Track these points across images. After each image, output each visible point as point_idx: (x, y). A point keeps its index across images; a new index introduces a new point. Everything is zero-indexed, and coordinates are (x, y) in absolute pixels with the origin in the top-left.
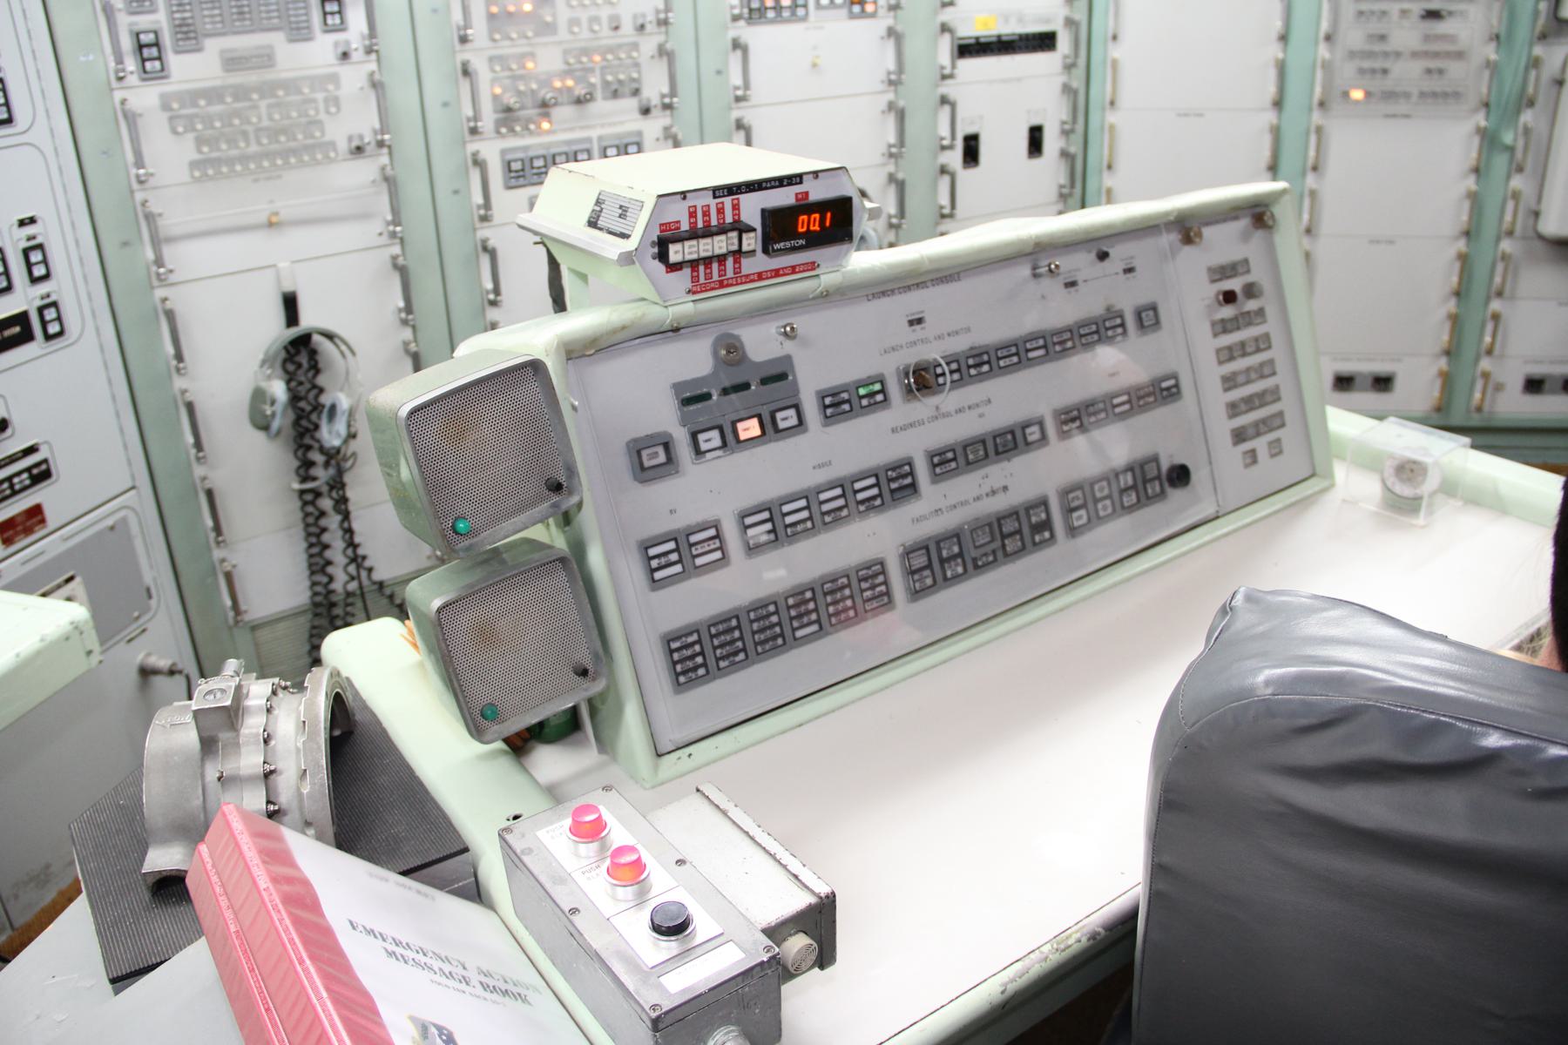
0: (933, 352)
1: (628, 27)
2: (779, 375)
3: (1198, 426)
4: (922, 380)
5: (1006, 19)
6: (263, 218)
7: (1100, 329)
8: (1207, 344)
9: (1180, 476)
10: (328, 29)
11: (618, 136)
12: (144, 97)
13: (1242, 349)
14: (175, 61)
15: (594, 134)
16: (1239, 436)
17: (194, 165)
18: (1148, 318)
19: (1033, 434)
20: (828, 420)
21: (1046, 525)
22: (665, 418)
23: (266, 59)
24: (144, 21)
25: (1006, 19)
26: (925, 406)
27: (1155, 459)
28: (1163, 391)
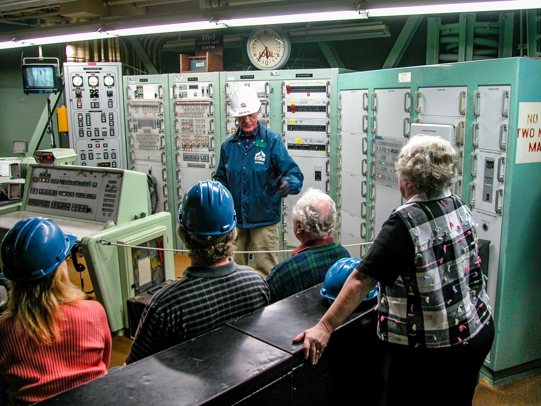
0: (65, 179)
1: (207, 133)
2: (49, 175)
3: (95, 205)
4: (63, 182)
5: (306, 140)
6: (146, 158)
7: (87, 184)
8: (104, 192)
9: (89, 210)
10: (158, 127)
11: (204, 154)
12: (134, 134)
13: (110, 196)
14: (138, 130)
15: (200, 153)
16: (103, 209)
17: (139, 146)
18: (95, 186)
19: (72, 194)
20: (51, 182)
21: (69, 207)
22: (38, 176)
23: (149, 131)
24: (135, 123)
25: (306, 140)
26: (62, 185)
27: (88, 206)
28: (91, 196)
